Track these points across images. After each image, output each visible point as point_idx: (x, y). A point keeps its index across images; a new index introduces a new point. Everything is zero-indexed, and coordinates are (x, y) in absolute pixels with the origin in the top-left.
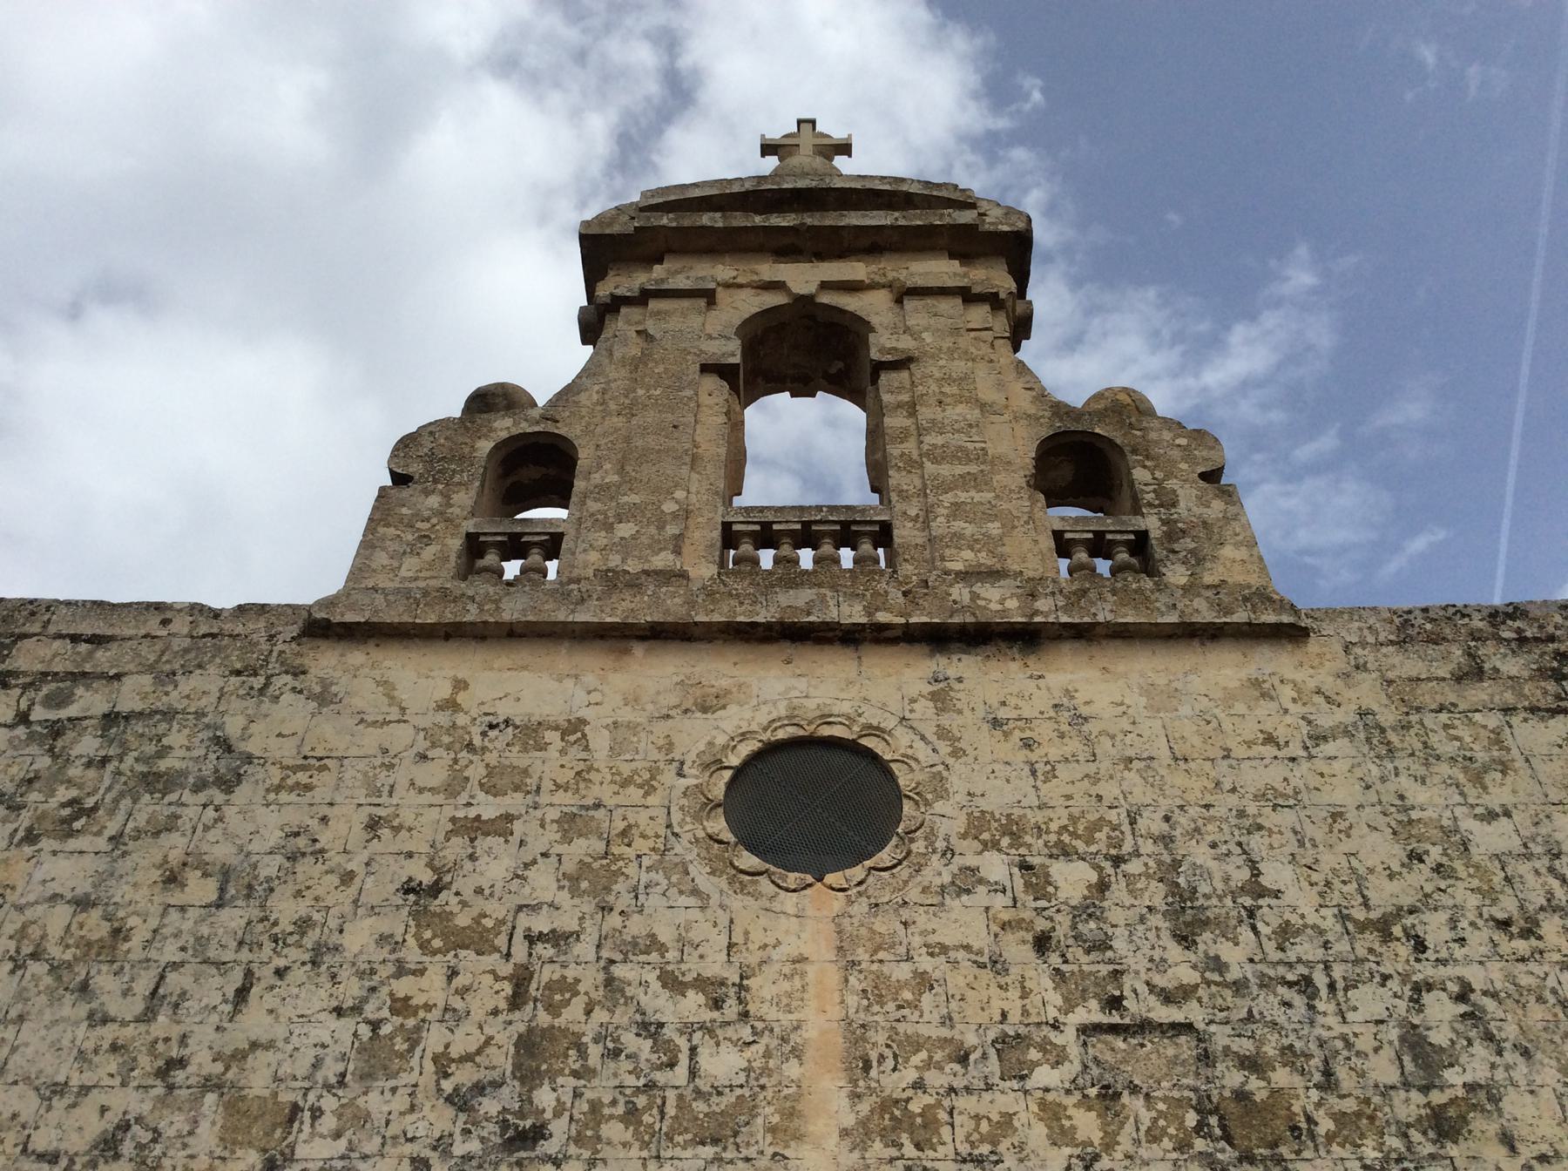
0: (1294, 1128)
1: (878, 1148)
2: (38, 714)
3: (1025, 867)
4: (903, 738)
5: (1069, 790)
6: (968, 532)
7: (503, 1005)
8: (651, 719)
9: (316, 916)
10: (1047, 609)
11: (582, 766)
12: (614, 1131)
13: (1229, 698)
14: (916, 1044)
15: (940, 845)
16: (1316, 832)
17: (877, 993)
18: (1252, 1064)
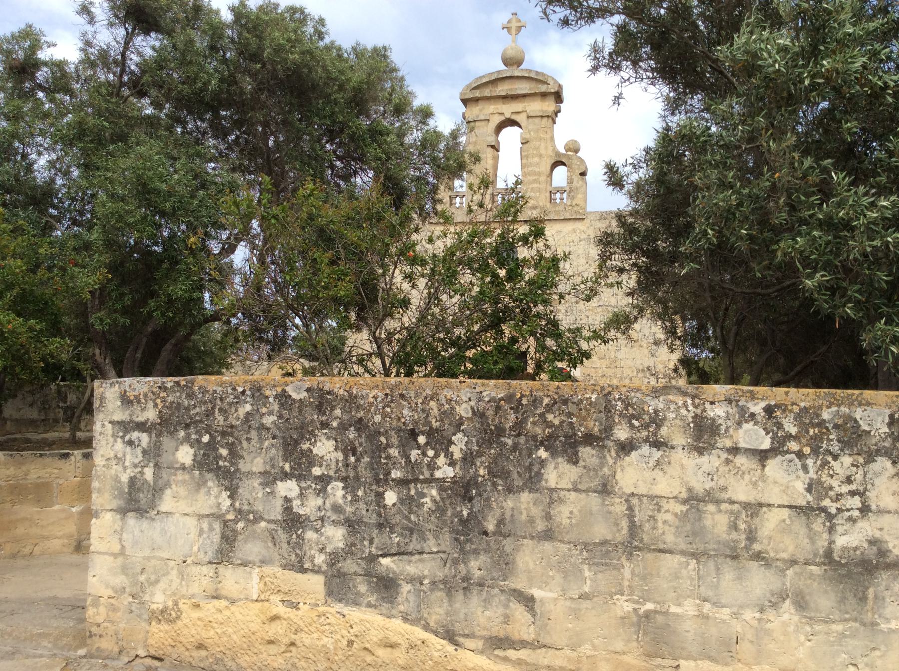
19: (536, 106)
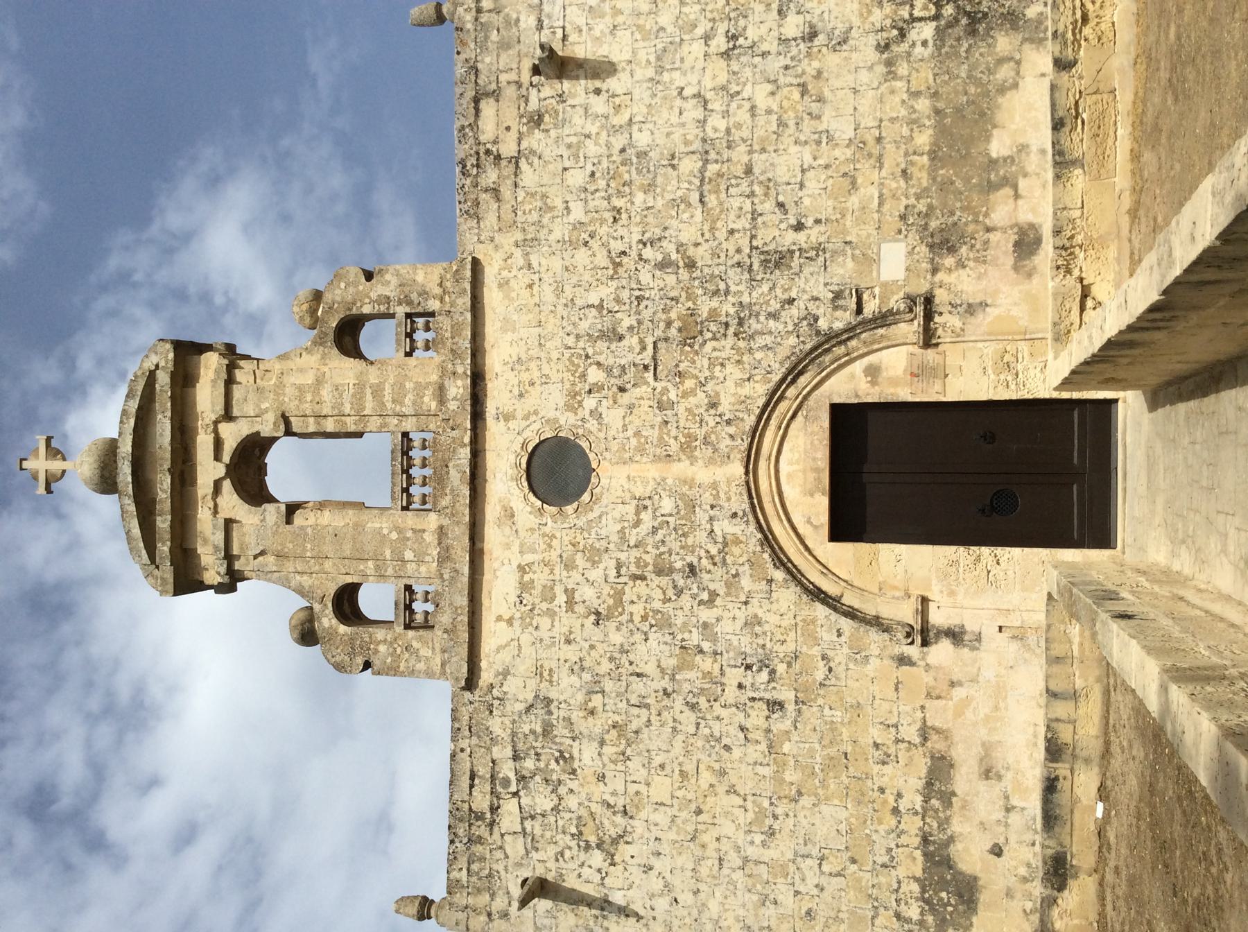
0: (691, 315)
1: (697, 453)
2: (513, 789)
3: (590, 392)
4: (527, 434)
5: (554, 371)
6: (412, 398)
7: (645, 583)
8: (518, 537)
9: (608, 655)
10: (464, 367)
11: (542, 564)
12: (690, 541)
13: (507, 297)
14: (661, 439)
15: (580, 423)
16: (574, 280)
17: (641, 450)
18: (669, 324)
19: (207, 398)
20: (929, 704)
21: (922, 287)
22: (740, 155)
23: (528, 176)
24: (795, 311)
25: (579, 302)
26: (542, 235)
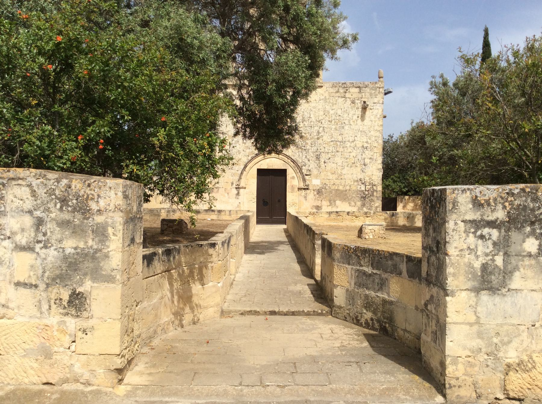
18: (305, 133)
20: (224, 189)
21: (310, 188)
22: (341, 149)
23: (341, 100)
24: (307, 161)
25: (311, 112)
26: (327, 103)
